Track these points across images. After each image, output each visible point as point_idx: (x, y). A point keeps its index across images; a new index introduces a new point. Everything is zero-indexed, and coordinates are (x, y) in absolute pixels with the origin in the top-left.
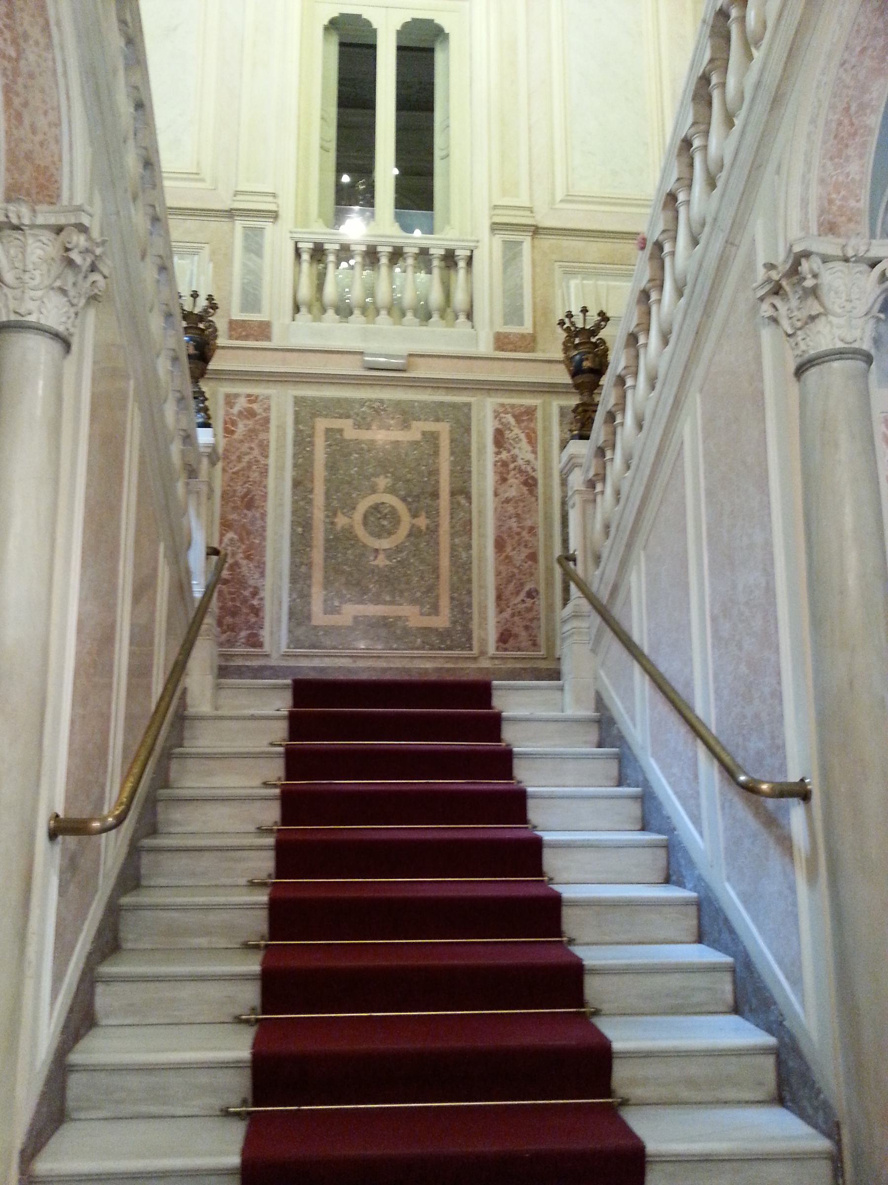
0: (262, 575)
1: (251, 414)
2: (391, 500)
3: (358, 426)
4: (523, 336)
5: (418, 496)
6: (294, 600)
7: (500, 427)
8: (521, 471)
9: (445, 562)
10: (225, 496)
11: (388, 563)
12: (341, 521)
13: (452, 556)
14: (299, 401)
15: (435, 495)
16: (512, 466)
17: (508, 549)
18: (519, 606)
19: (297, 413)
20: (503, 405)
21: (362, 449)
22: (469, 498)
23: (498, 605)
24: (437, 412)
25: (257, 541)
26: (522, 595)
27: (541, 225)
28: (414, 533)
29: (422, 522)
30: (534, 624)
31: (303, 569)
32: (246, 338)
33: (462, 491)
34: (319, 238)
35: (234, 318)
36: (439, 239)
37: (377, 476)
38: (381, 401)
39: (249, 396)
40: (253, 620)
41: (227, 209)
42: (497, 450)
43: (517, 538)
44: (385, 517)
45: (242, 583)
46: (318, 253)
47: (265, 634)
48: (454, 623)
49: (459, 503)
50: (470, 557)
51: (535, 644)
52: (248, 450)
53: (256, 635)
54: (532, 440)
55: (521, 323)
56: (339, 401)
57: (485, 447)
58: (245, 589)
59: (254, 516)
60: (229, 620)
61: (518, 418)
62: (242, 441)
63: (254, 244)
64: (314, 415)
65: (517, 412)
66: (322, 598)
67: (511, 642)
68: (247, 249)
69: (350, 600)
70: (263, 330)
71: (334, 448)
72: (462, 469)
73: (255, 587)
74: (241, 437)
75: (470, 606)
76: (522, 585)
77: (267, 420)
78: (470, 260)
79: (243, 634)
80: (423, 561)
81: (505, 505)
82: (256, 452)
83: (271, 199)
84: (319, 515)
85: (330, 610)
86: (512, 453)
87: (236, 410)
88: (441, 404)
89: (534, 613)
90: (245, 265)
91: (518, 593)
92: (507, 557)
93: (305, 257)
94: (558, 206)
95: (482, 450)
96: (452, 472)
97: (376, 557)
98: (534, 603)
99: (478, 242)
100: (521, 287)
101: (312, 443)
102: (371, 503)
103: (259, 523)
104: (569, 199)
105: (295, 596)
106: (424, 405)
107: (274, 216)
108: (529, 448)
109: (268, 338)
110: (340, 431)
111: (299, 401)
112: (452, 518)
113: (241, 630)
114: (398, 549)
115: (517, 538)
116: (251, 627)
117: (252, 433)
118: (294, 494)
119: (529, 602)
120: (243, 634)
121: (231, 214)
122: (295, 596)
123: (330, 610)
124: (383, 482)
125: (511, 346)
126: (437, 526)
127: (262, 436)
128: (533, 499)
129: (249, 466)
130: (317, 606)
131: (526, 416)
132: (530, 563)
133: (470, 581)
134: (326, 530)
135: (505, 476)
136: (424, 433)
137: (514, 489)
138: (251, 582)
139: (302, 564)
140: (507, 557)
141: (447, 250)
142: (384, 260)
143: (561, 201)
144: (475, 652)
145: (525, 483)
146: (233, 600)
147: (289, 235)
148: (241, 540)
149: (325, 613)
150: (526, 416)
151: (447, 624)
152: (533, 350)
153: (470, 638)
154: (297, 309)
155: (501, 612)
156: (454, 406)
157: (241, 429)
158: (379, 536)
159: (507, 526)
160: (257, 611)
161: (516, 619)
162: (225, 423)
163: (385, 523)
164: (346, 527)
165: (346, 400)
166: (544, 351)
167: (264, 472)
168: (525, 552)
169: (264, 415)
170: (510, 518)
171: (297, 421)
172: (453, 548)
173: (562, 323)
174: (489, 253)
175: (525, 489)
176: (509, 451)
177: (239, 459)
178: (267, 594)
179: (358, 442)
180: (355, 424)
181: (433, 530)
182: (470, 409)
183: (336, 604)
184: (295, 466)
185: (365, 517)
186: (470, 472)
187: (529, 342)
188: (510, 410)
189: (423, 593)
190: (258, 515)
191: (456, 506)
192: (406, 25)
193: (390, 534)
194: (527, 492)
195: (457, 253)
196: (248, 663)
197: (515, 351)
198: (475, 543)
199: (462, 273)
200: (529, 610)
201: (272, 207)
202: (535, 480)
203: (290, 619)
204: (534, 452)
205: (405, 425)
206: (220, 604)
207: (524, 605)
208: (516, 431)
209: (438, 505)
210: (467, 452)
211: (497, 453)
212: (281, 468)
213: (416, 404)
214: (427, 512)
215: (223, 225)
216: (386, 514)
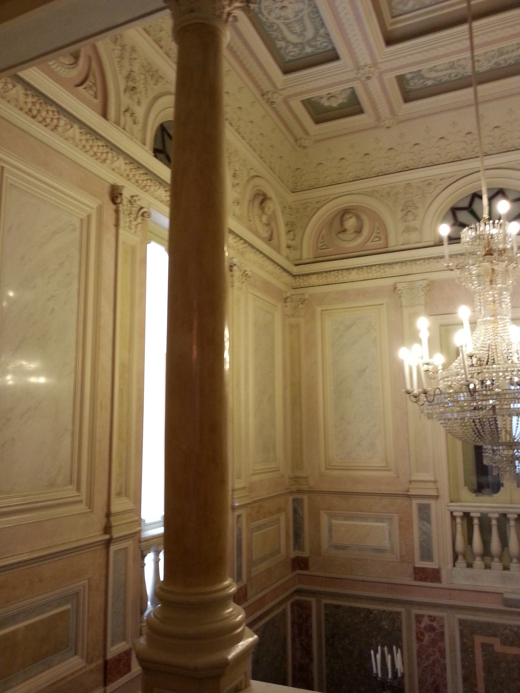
1: (432, 629)
14: (462, 622)
19: (461, 631)
32: (425, 580)
35: (417, 565)
39: (429, 616)
52: (432, 653)
70: (434, 575)
77: (442, 634)
82: (437, 655)
87: (423, 625)
90: (420, 529)
93: (458, 520)
101: (473, 652)
107: (437, 497)
110: (492, 646)
111: (462, 622)
117: (433, 643)
118: (464, 687)
157: (427, 638)
162: (417, 633)
165: (493, 624)
167: (444, 669)
169: (441, 630)
171: (462, 636)
180: (501, 642)
184: (463, 667)
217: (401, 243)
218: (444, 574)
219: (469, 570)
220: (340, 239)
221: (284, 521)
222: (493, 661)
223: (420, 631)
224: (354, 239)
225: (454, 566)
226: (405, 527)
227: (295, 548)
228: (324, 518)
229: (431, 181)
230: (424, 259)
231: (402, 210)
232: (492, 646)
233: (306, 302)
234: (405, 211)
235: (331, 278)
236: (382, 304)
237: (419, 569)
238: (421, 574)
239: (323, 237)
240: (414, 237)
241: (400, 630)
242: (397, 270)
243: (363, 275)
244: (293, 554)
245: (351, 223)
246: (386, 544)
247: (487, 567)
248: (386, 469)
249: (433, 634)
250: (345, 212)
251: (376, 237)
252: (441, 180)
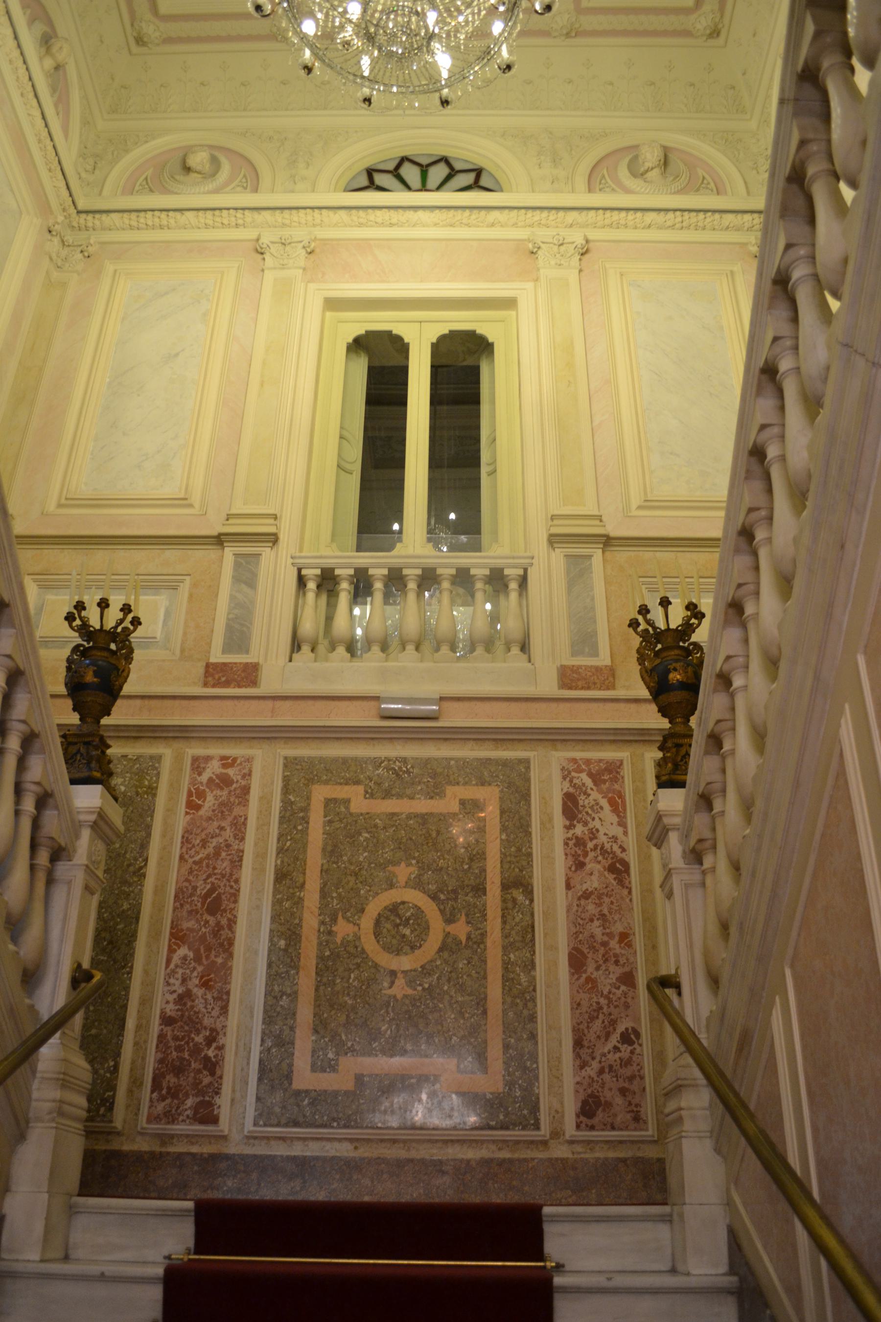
0: (224, 1010)
1: (224, 781)
2: (416, 897)
3: (370, 795)
4: (598, 669)
5: (454, 891)
6: (269, 1050)
7: (571, 790)
8: (604, 852)
9: (495, 991)
10: (179, 895)
11: (410, 992)
12: (343, 929)
13: (505, 979)
14: (289, 763)
15: (480, 890)
16: (590, 845)
17: (591, 968)
18: (610, 1056)
19: (286, 780)
20: (574, 761)
21: (376, 826)
22: (529, 892)
23: (577, 1056)
24: (480, 773)
25: (219, 960)
26: (614, 1039)
27: (613, 534)
28: (448, 946)
29: (461, 929)
30: (635, 1086)
31: (284, 1002)
32: (227, 684)
33: (518, 883)
34: (328, 563)
35: (213, 660)
36: (485, 557)
37: (396, 863)
38: (404, 760)
39: (223, 758)
40: (207, 1080)
41: (215, 533)
42: (568, 823)
43: (602, 950)
44: (406, 923)
45: (194, 1023)
46: (328, 581)
47: (224, 1103)
48: (510, 1084)
49: (514, 900)
50: (532, 981)
51: (637, 1118)
52: (217, 831)
53: (210, 1104)
54: (617, 806)
55: (595, 654)
56: (345, 761)
57: (551, 820)
58: (198, 1032)
59: (218, 924)
60: (171, 1079)
61: (597, 779)
62: (210, 819)
63: (246, 573)
64: (310, 781)
65: (594, 769)
66: (309, 1046)
67: (600, 1115)
68: (237, 579)
69: (352, 1050)
71: (337, 825)
72: (519, 850)
73: (213, 1030)
74: (210, 813)
75: (534, 1057)
76: (613, 1023)
77: (246, 790)
78: (523, 581)
79: (190, 1102)
80: (461, 988)
81: (583, 902)
82: (228, 833)
83: (272, 521)
84: (310, 922)
85: (321, 1065)
86: (590, 826)
87: (205, 777)
88: (489, 760)
89: (635, 1067)
90: (232, 598)
91: (608, 1035)
92: (589, 980)
93: (311, 585)
94: (635, 513)
95: (547, 823)
96: (504, 856)
97: (392, 983)
98: (632, 1052)
99: (533, 558)
100: (593, 609)
101: (306, 820)
102: (387, 903)
103: (225, 933)
104: (648, 504)
105: (269, 1043)
106: (463, 764)
107: (273, 539)
108: (615, 819)
109: (254, 683)
110: (347, 802)
111: (289, 763)
112: (504, 922)
113: (187, 1096)
114: (426, 970)
115: (602, 950)
116: (201, 1092)
117: (224, 808)
118: (276, 891)
119: (626, 1049)
120: (190, 1102)
121: (219, 540)
122: (269, 1043)
123: (321, 1065)
124: (404, 872)
125: (580, 683)
126: (483, 935)
127: (237, 811)
128: (625, 892)
129: (217, 853)
130: (302, 1061)
131: (608, 774)
132: (623, 988)
133: (533, 1018)
134: (320, 944)
135: (581, 859)
136: (463, 803)
137: (595, 877)
138: (207, 1021)
139: (283, 993)
140: (589, 980)
141: (492, 570)
142: (412, 585)
143: (640, 507)
144: (545, 1130)
145: (612, 869)
146: (179, 1049)
147: (290, 561)
148: (198, 959)
149: (314, 1069)
150: (608, 774)
151: (500, 1087)
152: (613, 687)
153: (535, 1109)
154: (296, 645)
155: (582, 1067)
156: (505, 763)
157: (210, 802)
158: (398, 952)
159: (586, 934)
160: (212, 1066)
161: (606, 1077)
162: (190, 794)
163: (407, 932)
164: (350, 938)
165: (355, 759)
166: (628, 688)
167: (237, 862)
168: (616, 972)
169: (243, 783)
170: (592, 920)
171: (286, 789)
172: (507, 966)
173: (634, 624)
174: (548, 569)
175: (611, 877)
176: (586, 824)
177: (204, 843)
178: (230, 1041)
179: (368, 816)
180: (366, 792)
181: (478, 941)
182: (528, 768)
183: (331, 1055)
184: (280, 851)
185: (377, 923)
186: (530, 855)
187: (606, 677)
188: (583, 767)
189: (462, 1038)
190: (224, 922)
191: (510, 905)
192: (443, 339)
193: (413, 948)
194: (615, 883)
195: (507, 572)
196: (194, 1149)
197: (588, 688)
198: (539, 959)
199: (514, 596)
200: (627, 1063)
201: (272, 530)
202: (626, 865)
203: (260, 1079)
204: (622, 824)
205: (435, 792)
206: (160, 1055)
207: (618, 1055)
208: (595, 795)
209: (485, 905)
210: (525, 828)
211: (568, 828)
212: (261, 856)
213: (452, 762)
214: (467, 915)
215: (210, 553)
216: (408, 920)
222: (345, 828)
223: (197, 789)
225: (290, 661)
232: (347, 802)
237: (216, 665)
241: (152, 791)
248: (183, 502)
249: (225, 793)
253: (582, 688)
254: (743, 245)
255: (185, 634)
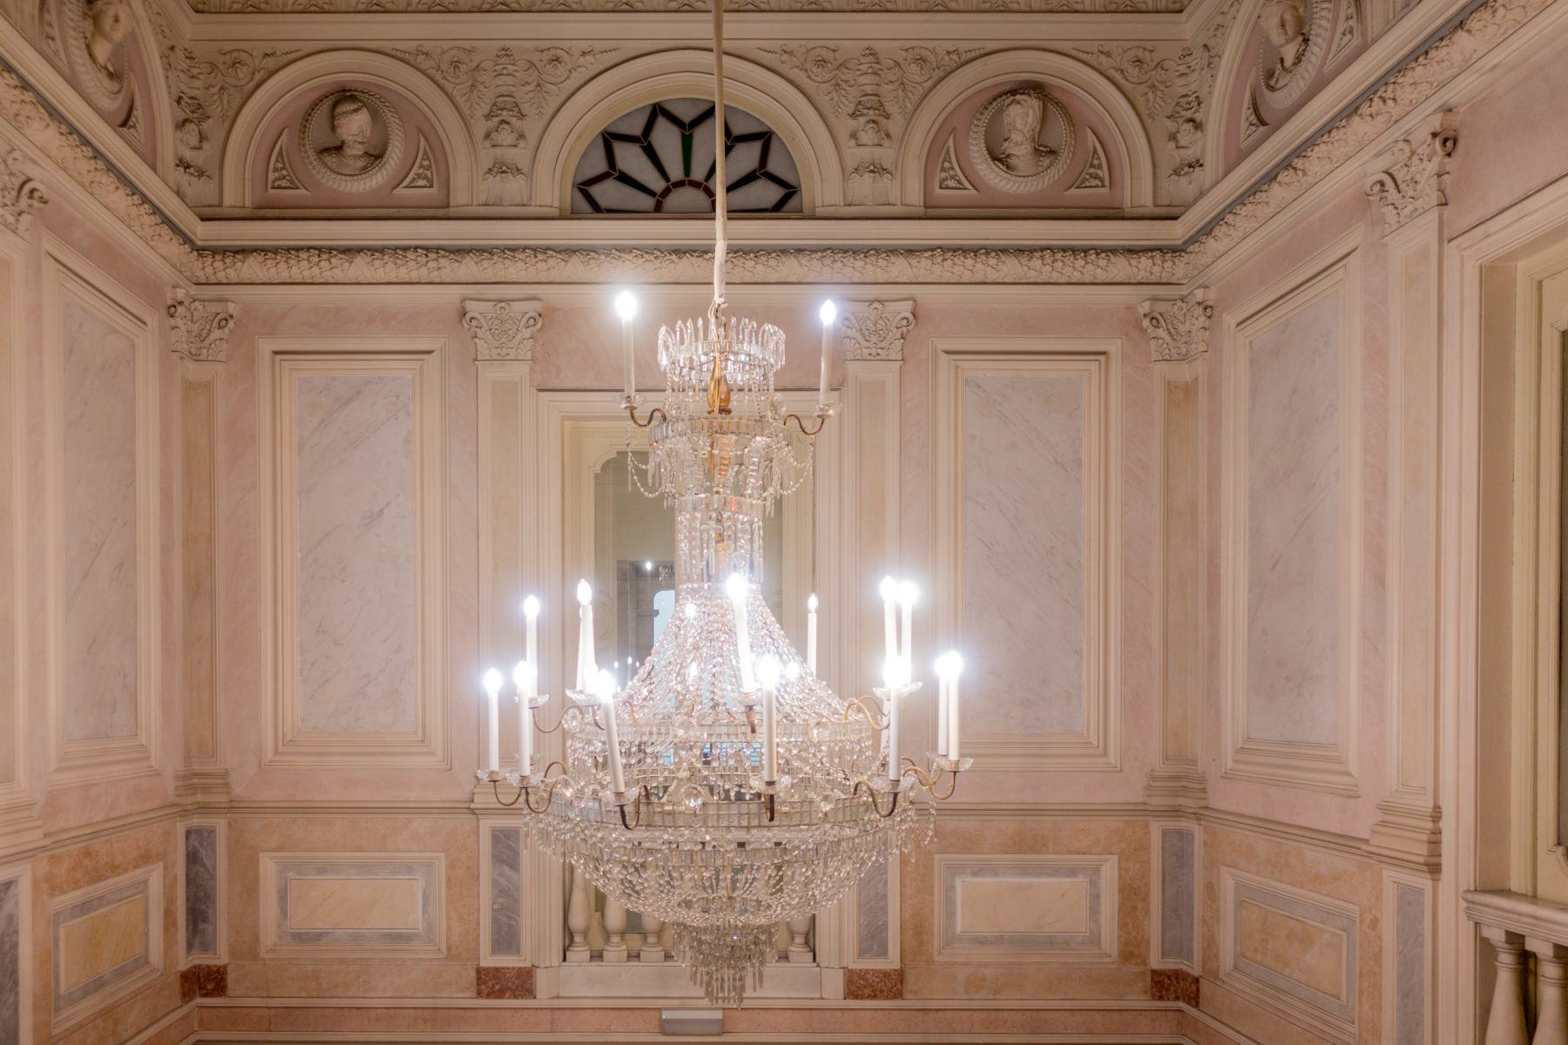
4: (886, 974)
32: (500, 994)
35: (484, 964)
55: (883, 953)
68: (498, 859)
70: (521, 983)
90: (495, 883)
100: (885, 896)
125: (867, 991)
152: (899, 995)
197: (875, 997)
217: (483, 199)
218: (542, 980)
219: (595, 967)
220: (326, 165)
221: (159, 884)
224: (364, 170)
225: (564, 959)
226: (462, 881)
227: (190, 947)
228: (268, 867)
229: (559, 52)
230: (535, 250)
231: (488, 117)
233: (231, 324)
234: (496, 120)
235: (300, 269)
236: (431, 352)
237: (487, 970)
238: (492, 983)
239: (280, 153)
240: (512, 188)
242: (468, 268)
243: (386, 269)
244: (184, 963)
245: (355, 125)
246: (415, 920)
247: (634, 956)
250: (344, 96)
251: (419, 176)
252: (584, 54)
253: (869, 997)
254: (1130, 308)
255: (449, 928)
